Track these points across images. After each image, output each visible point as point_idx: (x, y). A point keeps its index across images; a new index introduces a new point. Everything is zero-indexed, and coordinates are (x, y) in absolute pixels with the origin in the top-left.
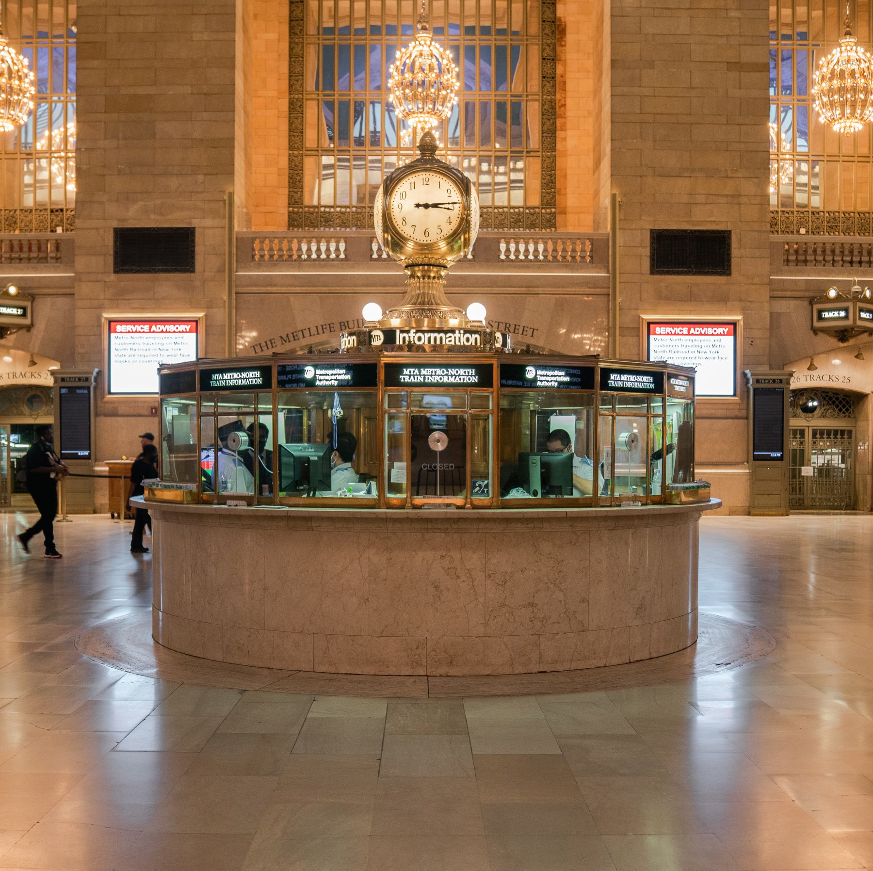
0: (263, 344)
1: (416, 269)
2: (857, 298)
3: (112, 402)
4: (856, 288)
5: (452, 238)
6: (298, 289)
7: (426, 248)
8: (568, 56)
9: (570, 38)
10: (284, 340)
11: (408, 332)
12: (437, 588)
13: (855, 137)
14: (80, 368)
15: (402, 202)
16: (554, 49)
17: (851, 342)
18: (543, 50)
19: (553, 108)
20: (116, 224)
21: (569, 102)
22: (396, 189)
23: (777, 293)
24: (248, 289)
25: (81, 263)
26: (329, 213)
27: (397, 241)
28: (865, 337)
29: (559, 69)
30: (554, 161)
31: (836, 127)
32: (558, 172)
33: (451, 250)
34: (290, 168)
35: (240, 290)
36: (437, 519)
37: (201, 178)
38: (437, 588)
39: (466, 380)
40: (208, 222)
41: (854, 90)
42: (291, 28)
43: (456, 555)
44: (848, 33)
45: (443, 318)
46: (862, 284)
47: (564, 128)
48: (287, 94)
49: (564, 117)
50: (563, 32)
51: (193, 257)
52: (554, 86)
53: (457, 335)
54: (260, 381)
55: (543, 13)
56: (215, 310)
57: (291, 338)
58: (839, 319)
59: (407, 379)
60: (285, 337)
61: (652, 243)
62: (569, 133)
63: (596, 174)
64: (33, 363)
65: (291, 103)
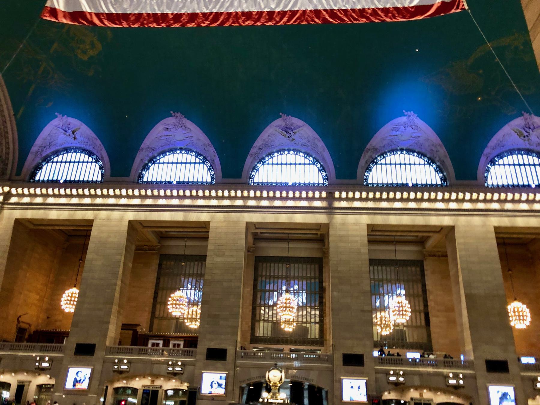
5: (279, 382)
10: (248, 380)
14: (195, 385)
23: (377, 372)
27: (270, 382)
28: (402, 386)
29: (324, 301)
40: (231, 347)
64: (182, 383)
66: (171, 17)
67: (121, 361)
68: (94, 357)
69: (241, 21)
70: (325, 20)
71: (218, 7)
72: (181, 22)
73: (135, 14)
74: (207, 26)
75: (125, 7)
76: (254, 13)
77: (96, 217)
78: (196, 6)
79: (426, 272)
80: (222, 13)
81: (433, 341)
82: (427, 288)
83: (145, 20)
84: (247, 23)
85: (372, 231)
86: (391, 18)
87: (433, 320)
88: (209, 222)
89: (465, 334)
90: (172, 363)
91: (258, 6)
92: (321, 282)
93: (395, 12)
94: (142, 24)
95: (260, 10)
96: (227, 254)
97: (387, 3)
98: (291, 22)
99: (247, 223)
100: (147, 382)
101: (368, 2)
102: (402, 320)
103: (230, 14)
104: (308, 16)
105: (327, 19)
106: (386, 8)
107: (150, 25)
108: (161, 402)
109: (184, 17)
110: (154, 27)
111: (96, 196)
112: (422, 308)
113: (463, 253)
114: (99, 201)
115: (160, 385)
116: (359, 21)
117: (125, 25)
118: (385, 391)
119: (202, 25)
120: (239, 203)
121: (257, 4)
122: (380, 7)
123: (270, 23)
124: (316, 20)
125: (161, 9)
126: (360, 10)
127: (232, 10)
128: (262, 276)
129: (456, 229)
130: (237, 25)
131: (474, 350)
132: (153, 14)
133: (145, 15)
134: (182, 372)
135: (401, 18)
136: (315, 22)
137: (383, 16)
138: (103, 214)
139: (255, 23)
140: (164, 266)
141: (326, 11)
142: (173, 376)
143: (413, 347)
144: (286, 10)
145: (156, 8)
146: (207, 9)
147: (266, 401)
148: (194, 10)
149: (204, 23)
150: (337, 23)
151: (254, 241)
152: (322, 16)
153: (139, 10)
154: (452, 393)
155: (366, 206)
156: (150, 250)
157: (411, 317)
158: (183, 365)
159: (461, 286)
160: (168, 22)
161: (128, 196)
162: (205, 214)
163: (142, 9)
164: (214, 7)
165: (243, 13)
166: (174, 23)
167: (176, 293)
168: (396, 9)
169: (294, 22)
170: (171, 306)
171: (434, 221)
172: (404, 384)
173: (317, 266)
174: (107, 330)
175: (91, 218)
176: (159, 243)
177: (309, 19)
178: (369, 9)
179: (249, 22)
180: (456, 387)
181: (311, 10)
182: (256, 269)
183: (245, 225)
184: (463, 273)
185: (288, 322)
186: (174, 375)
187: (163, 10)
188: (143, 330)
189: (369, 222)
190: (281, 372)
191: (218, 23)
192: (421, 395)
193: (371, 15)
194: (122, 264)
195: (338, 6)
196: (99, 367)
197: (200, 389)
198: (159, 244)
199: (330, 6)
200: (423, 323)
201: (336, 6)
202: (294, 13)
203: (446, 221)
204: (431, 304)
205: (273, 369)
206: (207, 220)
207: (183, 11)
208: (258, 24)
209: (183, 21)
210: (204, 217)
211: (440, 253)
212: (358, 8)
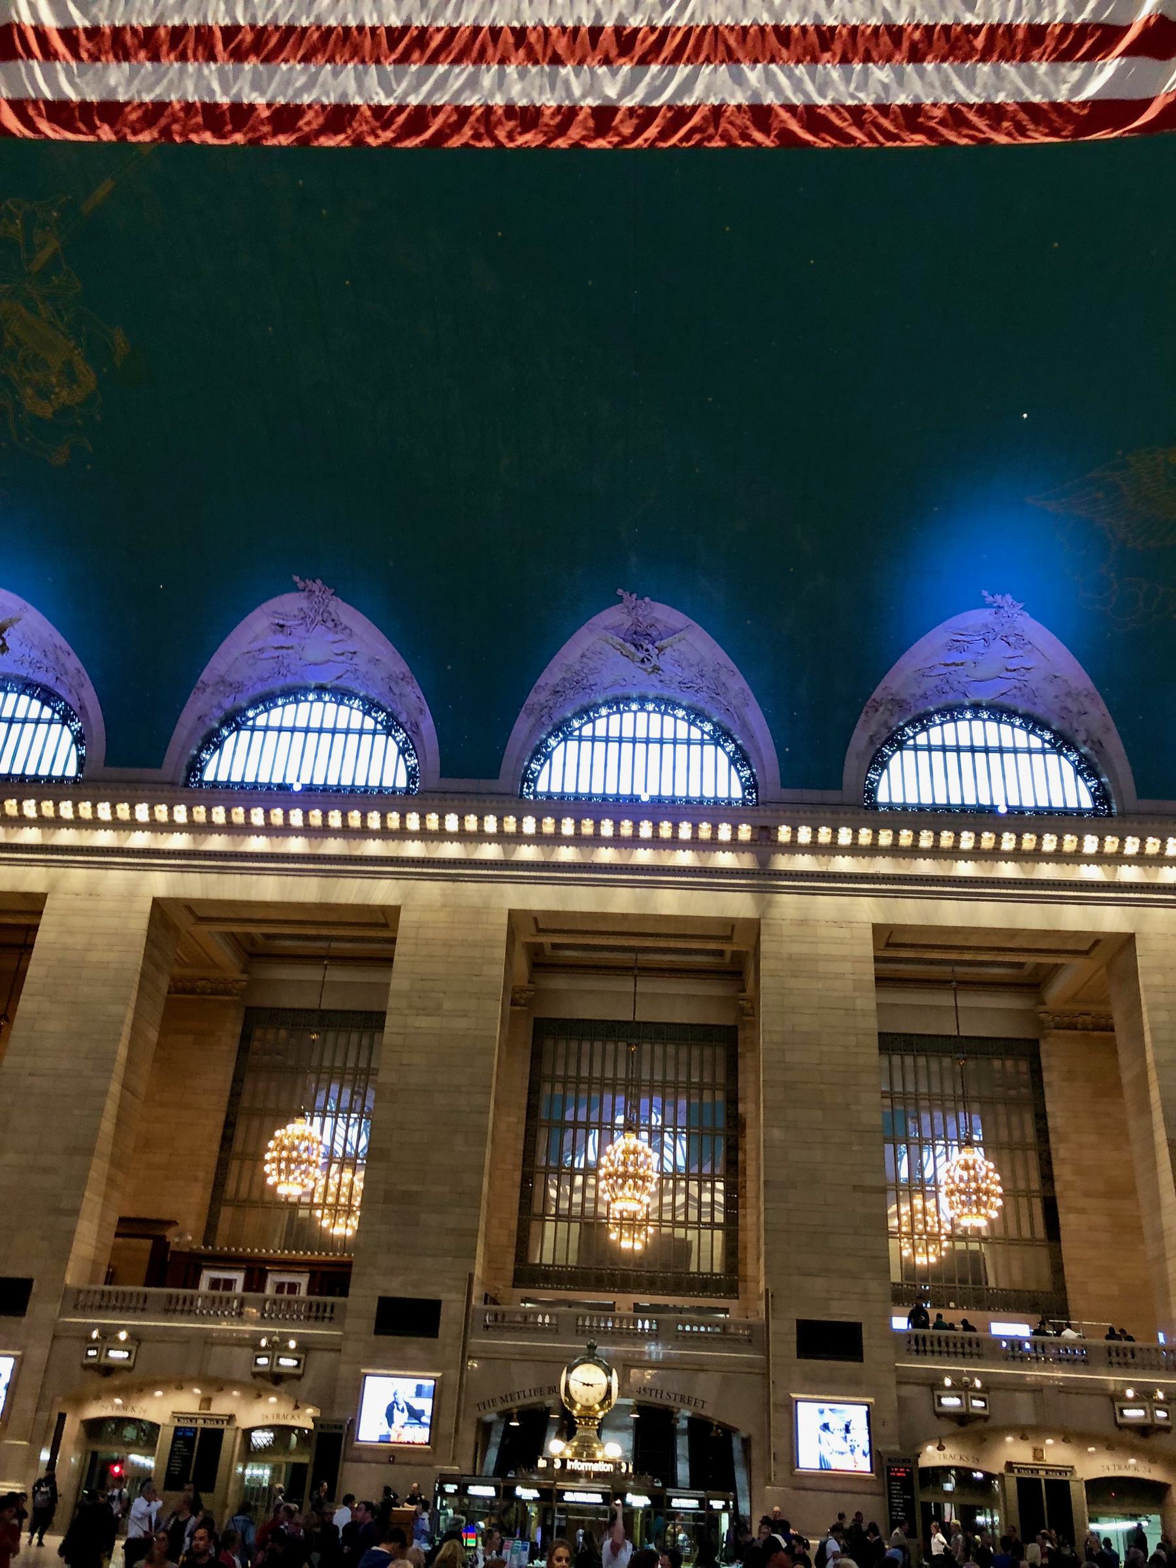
3: (359, 1449)
5: (601, 1403)
9: (748, 1131)
14: (337, 1415)
17: (969, 1427)
20: (381, 1294)
23: (903, 1378)
25: (350, 1324)
27: (573, 1403)
28: (980, 1425)
29: (740, 1157)
33: (602, 1408)
40: (453, 1296)
45: (593, 1455)
50: (744, 1127)
64: (297, 1407)
66: (266, 114)
67: (109, 1335)
68: (24, 1320)
69: (501, 134)
70: (786, 136)
71: (425, 89)
72: (300, 129)
73: (142, 104)
74: (385, 144)
75: (112, 81)
76: (548, 112)
77: (53, 887)
78: (352, 87)
79: (1046, 1077)
80: (437, 110)
81: (1069, 1287)
82: (1051, 1123)
83: (175, 120)
84: (521, 140)
85: (889, 945)
86: (1009, 134)
88: (396, 910)
90: (270, 1341)
91: (560, 91)
92: (733, 1100)
93: (1022, 116)
94: (166, 132)
95: (567, 103)
96: (447, 1005)
97: (998, 91)
98: (674, 140)
99: (511, 913)
100: (187, 1402)
101: (932, 86)
102: (976, 1221)
103: (464, 113)
104: (731, 123)
105: (793, 133)
106: (992, 104)
107: (194, 138)
108: (230, 1468)
109: (310, 115)
110: (204, 146)
111: (58, 822)
112: (1035, 1185)
113: (1162, 1016)
114: (66, 837)
115: (228, 1413)
116: (904, 141)
117: (106, 133)
118: (929, 1440)
119: (371, 140)
120: (490, 851)
121: (559, 84)
122: (973, 99)
123: (601, 143)
124: (758, 136)
125: (234, 91)
126: (903, 107)
127: (472, 100)
128: (553, 1079)
129: (1139, 944)
130: (487, 143)
132: (204, 104)
133: (177, 107)
134: (299, 1372)
135: (1046, 135)
136: (754, 141)
137: (985, 129)
138: (77, 877)
139: (550, 140)
140: (255, 1044)
141: (791, 108)
142: (270, 1385)
143: (1011, 1303)
144: (656, 103)
145: (216, 86)
146: (388, 95)
147: (558, 1465)
148: (344, 94)
149: (377, 136)
150: (826, 145)
151: (531, 973)
152: (775, 124)
153: (158, 90)
154: (1134, 1451)
155: (871, 871)
156: (215, 992)
157: (1002, 1211)
158: (305, 1349)
159: (1158, 1116)
160: (254, 129)
161: (154, 826)
162: (385, 884)
163: (168, 90)
164: (415, 88)
165: (510, 110)
166: (275, 134)
167: (290, 1127)
168: (1028, 107)
169: (681, 140)
170: (274, 1166)
171: (1074, 918)
172: (985, 1418)
173: (720, 1051)
174: (71, 1233)
175: (38, 888)
176: (243, 972)
177: (734, 133)
178: (934, 105)
179: (528, 137)
180: (1145, 1430)
181: (739, 107)
182: (536, 1057)
183: (505, 920)
184: (1159, 1078)
185: (631, 1223)
186: (276, 1379)
187: (239, 94)
188: (186, 1237)
189: (880, 920)
190: (608, 1373)
191: (427, 135)
192: (1038, 1453)
193: (943, 122)
194: (126, 1031)
195: (831, 95)
196: (38, 1354)
197: (353, 1425)
198: (245, 977)
199: (806, 94)
200: (1040, 1232)
201: (823, 95)
202: (680, 115)
203: (1110, 919)
205: (584, 1362)
206: (391, 902)
207: (306, 99)
208: (562, 143)
209: (306, 129)
210: (381, 892)
211: (1088, 1019)
212: (899, 102)
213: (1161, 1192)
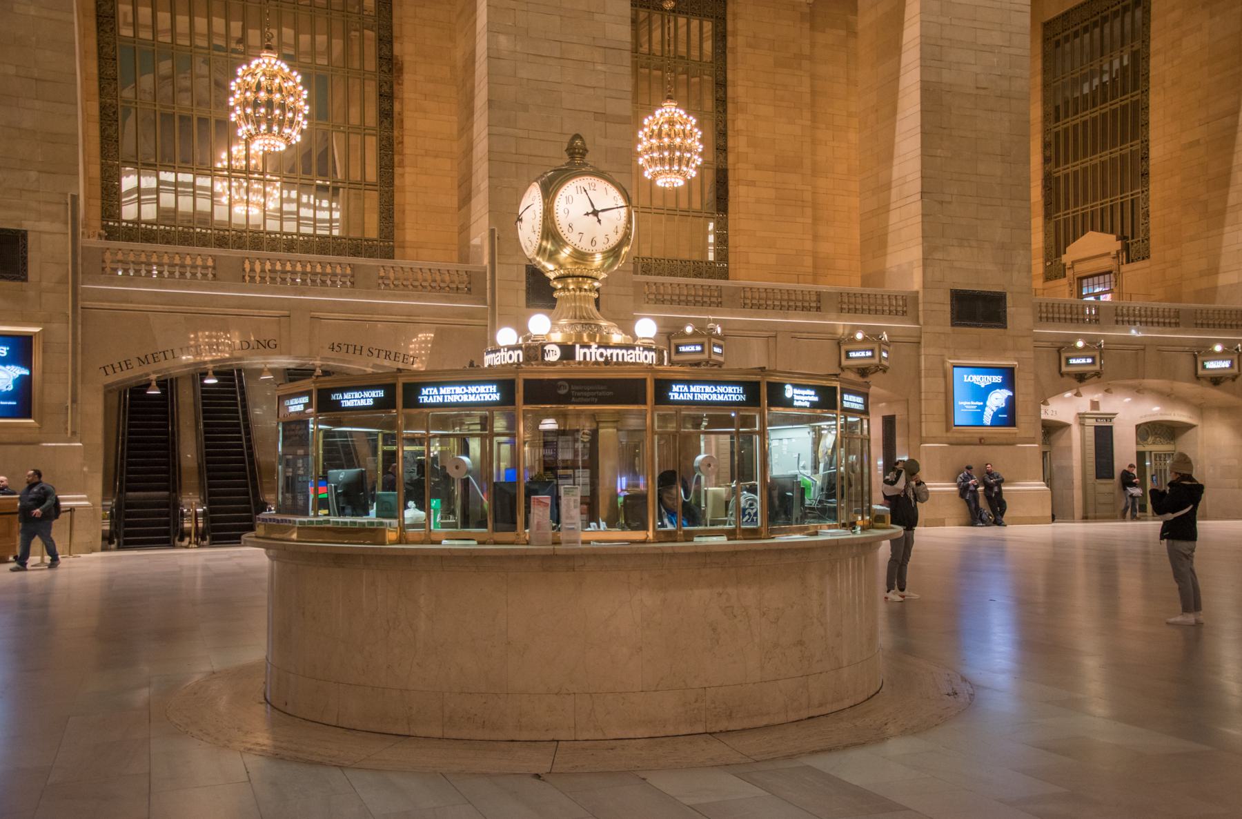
0: (116, 365)
1: (570, 280)
2: (711, 335)
4: (710, 325)
6: (160, 307)
7: (581, 256)
8: (406, 95)
9: (407, 77)
10: (142, 361)
11: (589, 347)
12: (714, 630)
13: (677, 191)
15: (568, 206)
16: (391, 87)
18: (381, 87)
19: (391, 145)
21: (406, 139)
22: (561, 192)
24: (97, 304)
26: (151, 230)
30: (392, 196)
31: (660, 182)
32: (396, 207)
34: (102, 178)
35: (87, 304)
36: (716, 553)
37: (33, 175)
38: (714, 630)
39: (735, 398)
40: (45, 225)
41: (671, 148)
42: (99, 25)
43: (732, 591)
44: (670, 98)
46: (715, 321)
47: (402, 165)
48: (97, 97)
49: (402, 154)
50: (401, 70)
51: (25, 264)
52: (392, 123)
53: (637, 352)
54: (497, 397)
55: (380, 49)
56: (55, 326)
57: (151, 359)
58: (695, 352)
59: (426, 400)
60: (143, 358)
61: (527, 278)
62: (408, 169)
63: (463, 211)
65: (103, 108)
87: (738, 193)
89: (894, 217)
131: (926, 261)
159: (911, 56)
204: (737, 144)
213: (897, 140)
